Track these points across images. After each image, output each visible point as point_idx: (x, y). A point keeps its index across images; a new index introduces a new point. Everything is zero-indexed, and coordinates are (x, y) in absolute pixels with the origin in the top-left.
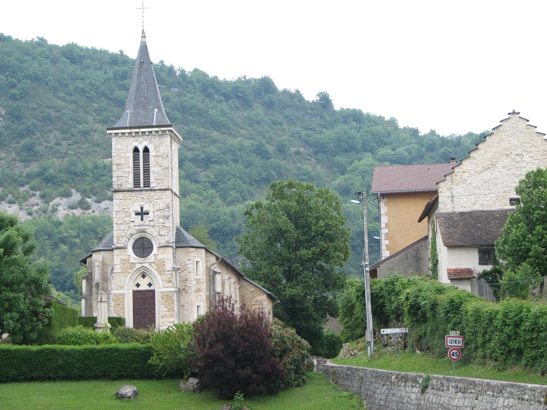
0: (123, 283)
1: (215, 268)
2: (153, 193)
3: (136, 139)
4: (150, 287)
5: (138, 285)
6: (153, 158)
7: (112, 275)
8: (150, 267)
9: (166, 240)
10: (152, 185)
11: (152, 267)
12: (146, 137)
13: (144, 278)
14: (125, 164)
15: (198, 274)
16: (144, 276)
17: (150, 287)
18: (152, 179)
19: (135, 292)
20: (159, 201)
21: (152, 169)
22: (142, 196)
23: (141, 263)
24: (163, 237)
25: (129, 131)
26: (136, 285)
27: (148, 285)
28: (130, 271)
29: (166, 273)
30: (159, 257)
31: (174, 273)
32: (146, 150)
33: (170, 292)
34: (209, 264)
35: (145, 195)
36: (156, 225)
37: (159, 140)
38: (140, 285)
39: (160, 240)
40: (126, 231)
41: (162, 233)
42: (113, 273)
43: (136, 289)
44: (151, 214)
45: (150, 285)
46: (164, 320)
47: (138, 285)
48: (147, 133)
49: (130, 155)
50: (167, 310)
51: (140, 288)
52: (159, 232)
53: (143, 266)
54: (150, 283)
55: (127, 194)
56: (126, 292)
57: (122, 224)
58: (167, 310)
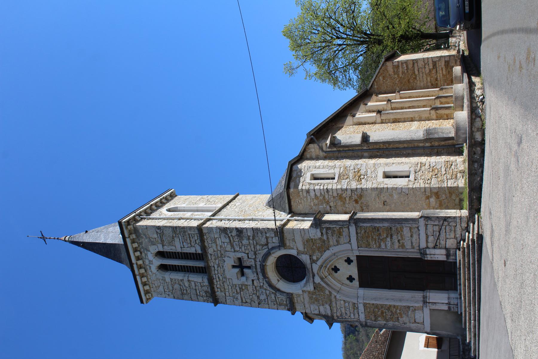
0: (347, 304)
1: (326, 144)
2: (210, 251)
3: (148, 267)
4: (352, 261)
5: (351, 279)
6: (165, 247)
7: (335, 318)
8: (319, 263)
9: (273, 235)
10: (199, 251)
11: (318, 259)
12: (143, 255)
13: (339, 270)
14: (180, 285)
15: (332, 176)
16: (336, 270)
17: (352, 261)
18: (192, 250)
19: (363, 285)
20: (219, 242)
21: (179, 250)
22: (216, 266)
24: (270, 240)
25: (138, 278)
27: (349, 264)
28: (327, 292)
30: (301, 248)
31: (324, 226)
32: (161, 254)
33: (357, 233)
34: (322, 154)
35: (213, 262)
36: (253, 249)
37: (142, 237)
38: (350, 276)
39: (274, 245)
40: (268, 292)
41: (263, 241)
42: (332, 316)
43: (356, 283)
44: (239, 255)
45: (349, 261)
46: (408, 245)
48: (138, 254)
49: (169, 276)
51: (355, 275)
52: (263, 246)
53: (318, 273)
54: (346, 261)
55: (217, 284)
57: (258, 297)
58: (389, 239)
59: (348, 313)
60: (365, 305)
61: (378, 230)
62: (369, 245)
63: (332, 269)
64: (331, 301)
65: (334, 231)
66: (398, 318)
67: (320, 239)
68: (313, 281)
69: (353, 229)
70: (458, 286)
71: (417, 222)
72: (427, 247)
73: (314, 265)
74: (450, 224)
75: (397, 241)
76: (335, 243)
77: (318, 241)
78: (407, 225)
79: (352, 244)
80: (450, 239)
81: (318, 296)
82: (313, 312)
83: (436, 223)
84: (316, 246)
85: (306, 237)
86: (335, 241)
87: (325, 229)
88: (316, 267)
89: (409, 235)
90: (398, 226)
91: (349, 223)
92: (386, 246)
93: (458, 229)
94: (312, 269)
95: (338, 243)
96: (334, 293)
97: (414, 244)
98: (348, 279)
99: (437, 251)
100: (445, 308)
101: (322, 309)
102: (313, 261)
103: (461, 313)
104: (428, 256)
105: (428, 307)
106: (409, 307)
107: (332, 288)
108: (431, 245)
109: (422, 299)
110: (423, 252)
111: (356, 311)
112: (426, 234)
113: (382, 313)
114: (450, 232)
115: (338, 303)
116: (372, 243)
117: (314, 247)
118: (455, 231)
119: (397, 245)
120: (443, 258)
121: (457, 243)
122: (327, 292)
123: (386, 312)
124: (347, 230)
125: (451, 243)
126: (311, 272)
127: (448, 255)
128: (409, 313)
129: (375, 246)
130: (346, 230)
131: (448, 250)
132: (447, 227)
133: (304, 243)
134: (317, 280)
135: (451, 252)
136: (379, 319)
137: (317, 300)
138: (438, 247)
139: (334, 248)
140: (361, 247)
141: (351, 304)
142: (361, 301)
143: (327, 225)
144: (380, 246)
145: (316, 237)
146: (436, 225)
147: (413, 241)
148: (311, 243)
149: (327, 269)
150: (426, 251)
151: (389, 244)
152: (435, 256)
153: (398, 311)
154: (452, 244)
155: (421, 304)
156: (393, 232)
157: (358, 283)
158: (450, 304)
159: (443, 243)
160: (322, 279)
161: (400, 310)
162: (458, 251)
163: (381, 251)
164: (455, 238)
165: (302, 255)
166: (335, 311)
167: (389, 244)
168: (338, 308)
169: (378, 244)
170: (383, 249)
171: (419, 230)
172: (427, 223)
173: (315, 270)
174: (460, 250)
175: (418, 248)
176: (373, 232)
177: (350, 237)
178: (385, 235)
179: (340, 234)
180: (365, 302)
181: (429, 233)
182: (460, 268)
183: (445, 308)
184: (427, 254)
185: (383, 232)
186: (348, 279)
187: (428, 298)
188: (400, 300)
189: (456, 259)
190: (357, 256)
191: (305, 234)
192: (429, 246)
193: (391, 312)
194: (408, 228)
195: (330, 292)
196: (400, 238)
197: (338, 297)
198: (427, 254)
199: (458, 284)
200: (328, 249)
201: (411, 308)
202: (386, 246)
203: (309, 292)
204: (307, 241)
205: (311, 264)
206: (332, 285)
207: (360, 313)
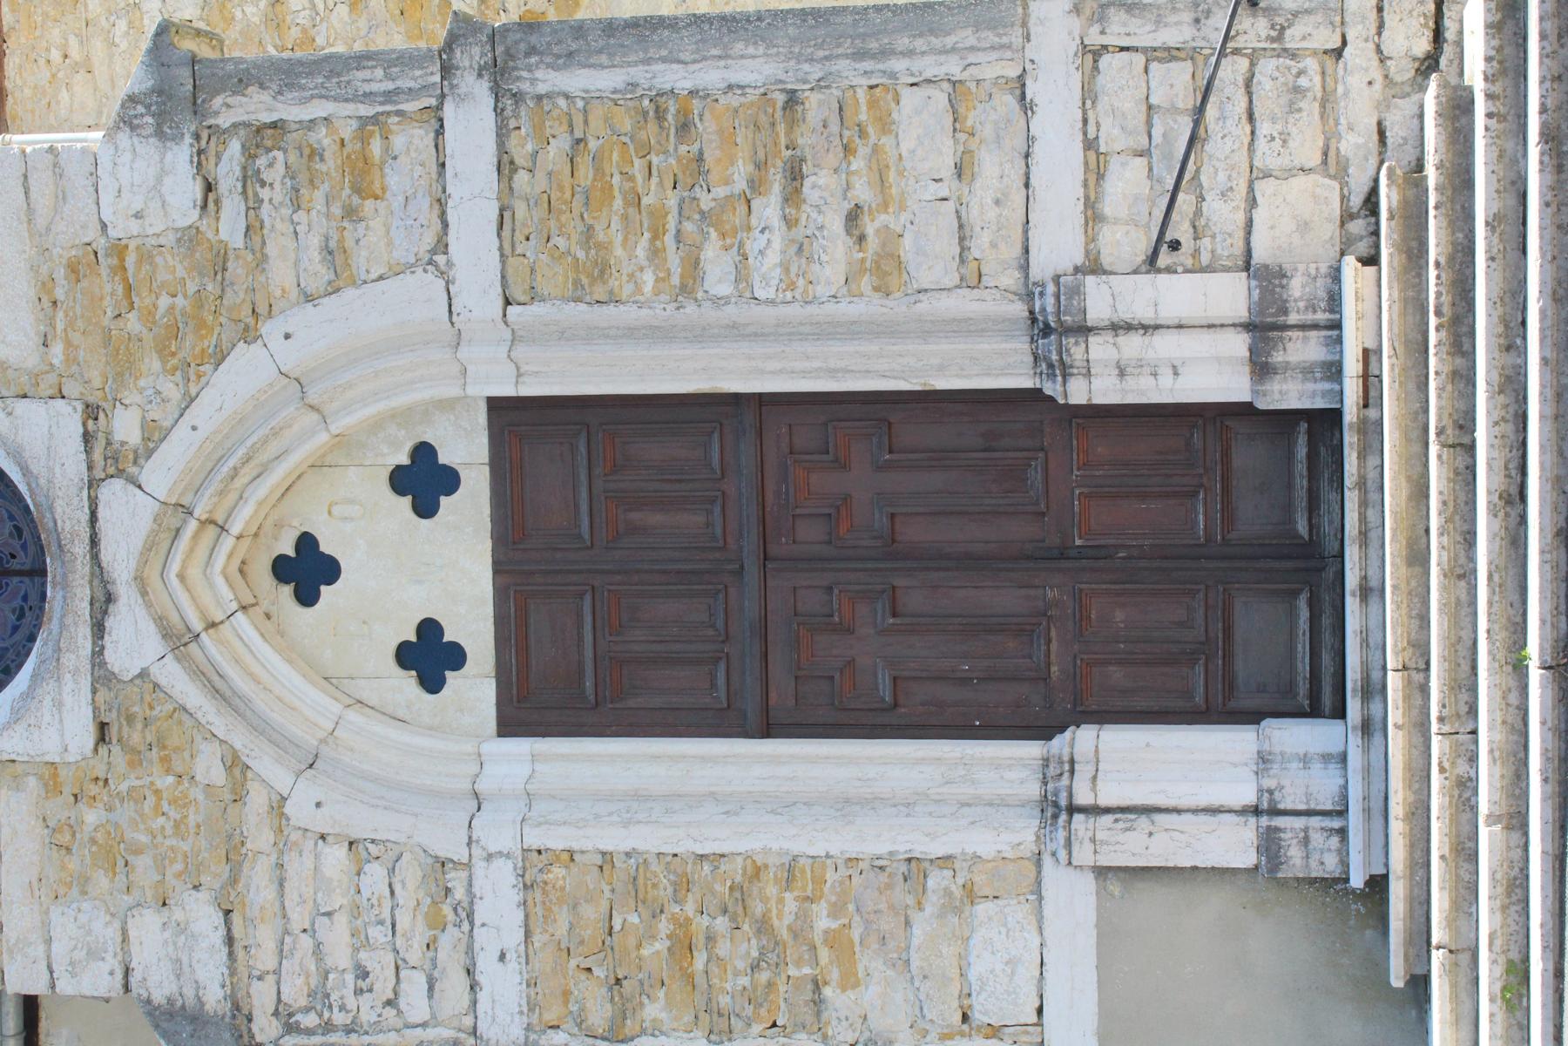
0: (375, 876)
4: (449, 480)
11: (154, 436)
13: (330, 570)
16: (307, 570)
17: (449, 480)
19: (525, 710)
23: (104, 602)
26: (432, 683)
27: (425, 509)
29: (230, 226)
31: (232, 110)
33: (505, 167)
38: (429, 629)
42: (239, 1012)
43: (475, 689)
45: (423, 481)
46: (930, 260)
47: (428, 656)
50: (769, 208)
51: (472, 625)
53: (141, 582)
54: (400, 480)
56: (498, 832)
58: (769, 208)
59: (380, 964)
60: (535, 872)
61: (685, 127)
62: (602, 270)
63: (282, 569)
64: (234, 855)
65: (315, 154)
66: (817, 986)
67: (190, 238)
68: (98, 652)
69: (471, 122)
70: (1352, 605)
71: (1016, 37)
72: (1093, 266)
73: (113, 493)
74: (1293, 38)
75: (836, 224)
76: (317, 273)
77: (172, 266)
78: (929, 67)
79: (461, 274)
80: (1289, 173)
81: (125, 813)
82: (65, 986)
83: (1171, 36)
84: (149, 316)
85: (73, 229)
86: (314, 254)
87: (235, 146)
88: (127, 517)
89: (945, 164)
90: (852, 73)
91: (447, 70)
92: (742, 275)
93: (1356, 81)
94: (94, 542)
95: (340, 269)
96: (271, 770)
97: (980, 245)
98: (405, 656)
99: (1177, 294)
100: (1234, 846)
101: (148, 929)
102: (108, 463)
103: (1378, 884)
104: (1100, 349)
105: (1084, 855)
106: (915, 869)
107: (261, 728)
108: (1124, 242)
109: (1034, 790)
110: (1053, 326)
111: (447, 940)
112: (1090, 144)
113: (683, 946)
114: (1292, 108)
115: (300, 867)
116: (631, 257)
117: (133, 323)
118: (1326, 101)
119: (835, 252)
120: (1211, 373)
121: (1347, 217)
122: (209, 767)
123: (711, 939)
124: (421, 137)
125: (1295, 219)
126: (82, 567)
127: (1264, 329)
128: (918, 932)
129: (648, 278)
130: (412, 141)
131: (1268, 280)
132: (1267, 66)
133: (47, 285)
134: (134, 643)
135: (1297, 288)
136: (653, 1010)
137: (114, 854)
138: (1184, 257)
139: (301, 319)
140: (534, 297)
141: (410, 873)
142: (498, 832)
143: (257, 106)
144: (689, 284)
145: (155, 224)
146: (1170, 54)
147: (973, 215)
148: (107, 286)
149: (228, 543)
150: (1077, 291)
151: (769, 250)
152: (1165, 346)
153: (823, 922)
154: (1304, 226)
155: (1024, 832)
156: (805, 140)
157: (487, 692)
158: (1275, 812)
159: (1224, 214)
160: (179, 639)
161: (836, 911)
162: (1350, 264)
163: (700, 335)
164: (1331, 163)
165: (21, 406)
166: (265, 959)
167: (773, 257)
168: (299, 918)
169: (674, 261)
170: (719, 301)
171: (1026, 105)
172: (1094, 38)
173: (120, 557)
174: (1372, 260)
175: (1011, 279)
176: (645, 151)
177: (441, 203)
178: (741, 172)
179: (363, 180)
180: (534, 839)
181: (1112, 136)
182: (1371, 431)
183: (1234, 846)
184: (1084, 330)
185: (728, 139)
186: (405, 656)
187: (1083, 772)
188: (846, 805)
189: (1334, 371)
190: (496, 406)
191: (61, 197)
192: (1106, 261)
193: (763, 927)
194: (940, 97)
195: (235, 765)
196: (863, 192)
197: (299, 810)
198: (1084, 330)
199: (1352, 580)
200: (249, 335)
201: (937, 880)
202: (742, 275)
203: (51, 776)
204: (73, 269)
205: (93, 484)
206: (260, 702)
207: (486, 964)
